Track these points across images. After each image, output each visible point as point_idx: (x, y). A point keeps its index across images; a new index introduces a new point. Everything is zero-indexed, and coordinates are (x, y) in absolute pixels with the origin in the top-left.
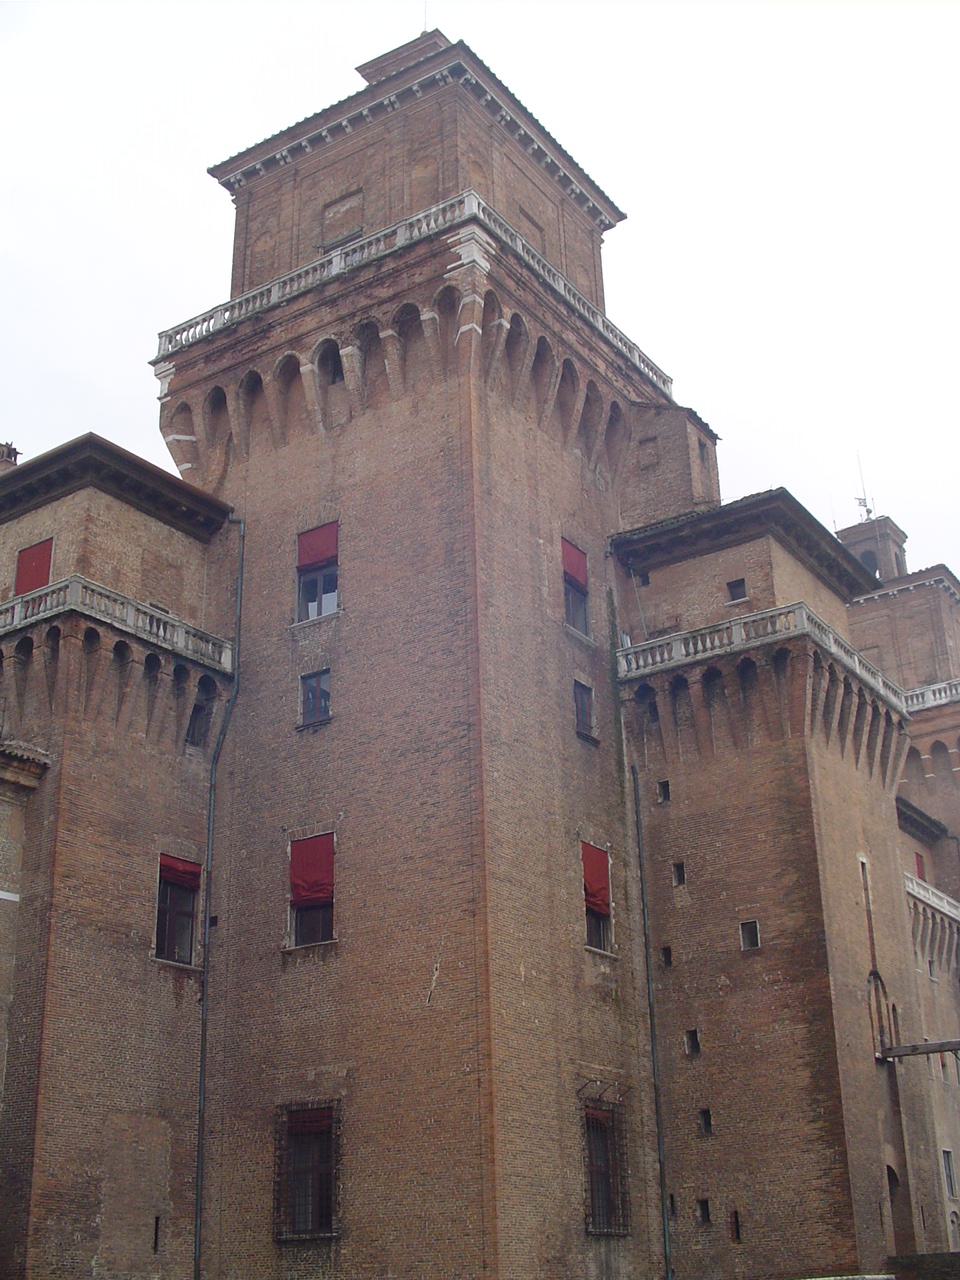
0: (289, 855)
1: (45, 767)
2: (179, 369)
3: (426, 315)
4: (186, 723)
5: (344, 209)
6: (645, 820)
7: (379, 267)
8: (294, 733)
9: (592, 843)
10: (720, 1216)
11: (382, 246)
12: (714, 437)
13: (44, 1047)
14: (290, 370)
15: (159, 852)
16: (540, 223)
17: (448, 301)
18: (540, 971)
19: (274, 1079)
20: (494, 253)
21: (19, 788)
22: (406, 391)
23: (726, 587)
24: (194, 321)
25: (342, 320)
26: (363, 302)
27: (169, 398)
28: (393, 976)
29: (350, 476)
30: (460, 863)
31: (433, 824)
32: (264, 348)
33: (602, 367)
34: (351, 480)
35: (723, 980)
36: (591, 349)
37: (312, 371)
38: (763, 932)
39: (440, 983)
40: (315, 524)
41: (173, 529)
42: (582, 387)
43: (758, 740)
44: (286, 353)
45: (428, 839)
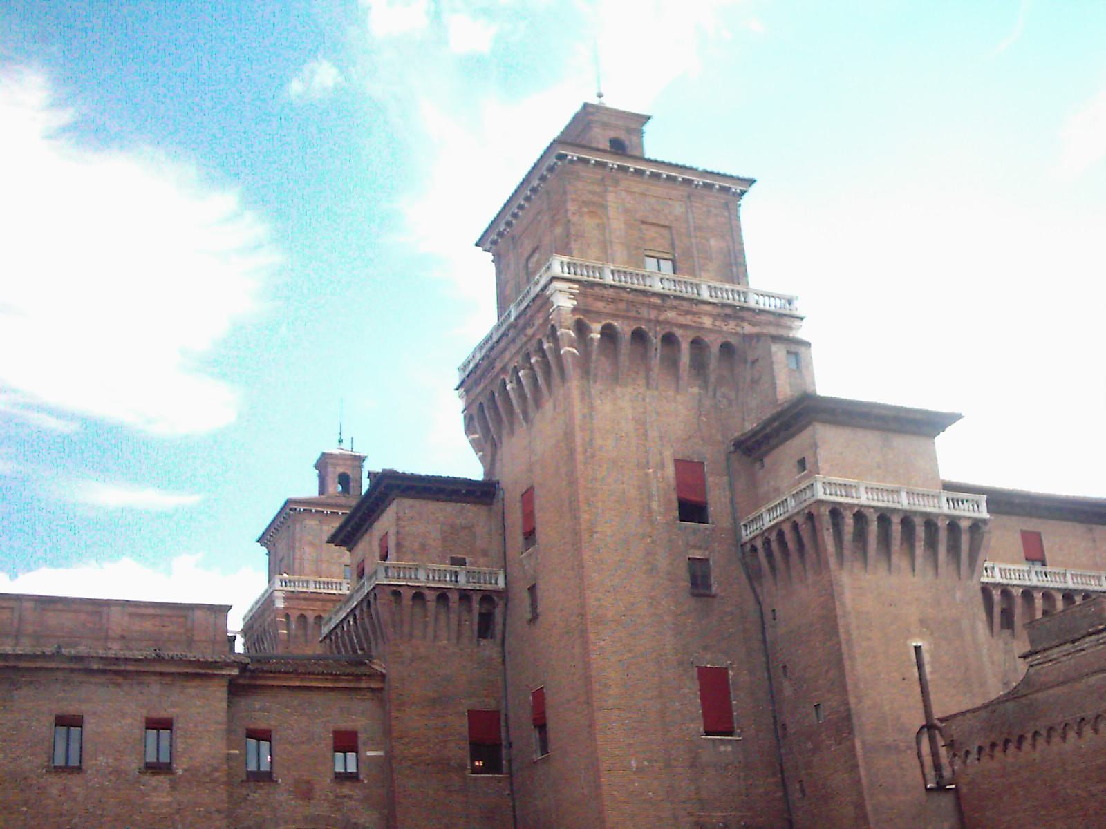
1: (383, 675)
2: (467, 392)
4: (476, 627)
9: (709, 666)
12: (808, 344)
15: (466, 710)
16: (667, 224)
18: (650, 760)
20: (578, 291)
21: (372, 690)
23: (796, 463)
26: (524, 339)
33: (707, 322)
36: (694, 314)
37: (513, 388)
41: (464, 505)
42: (685, 346)
44: (502, 377)
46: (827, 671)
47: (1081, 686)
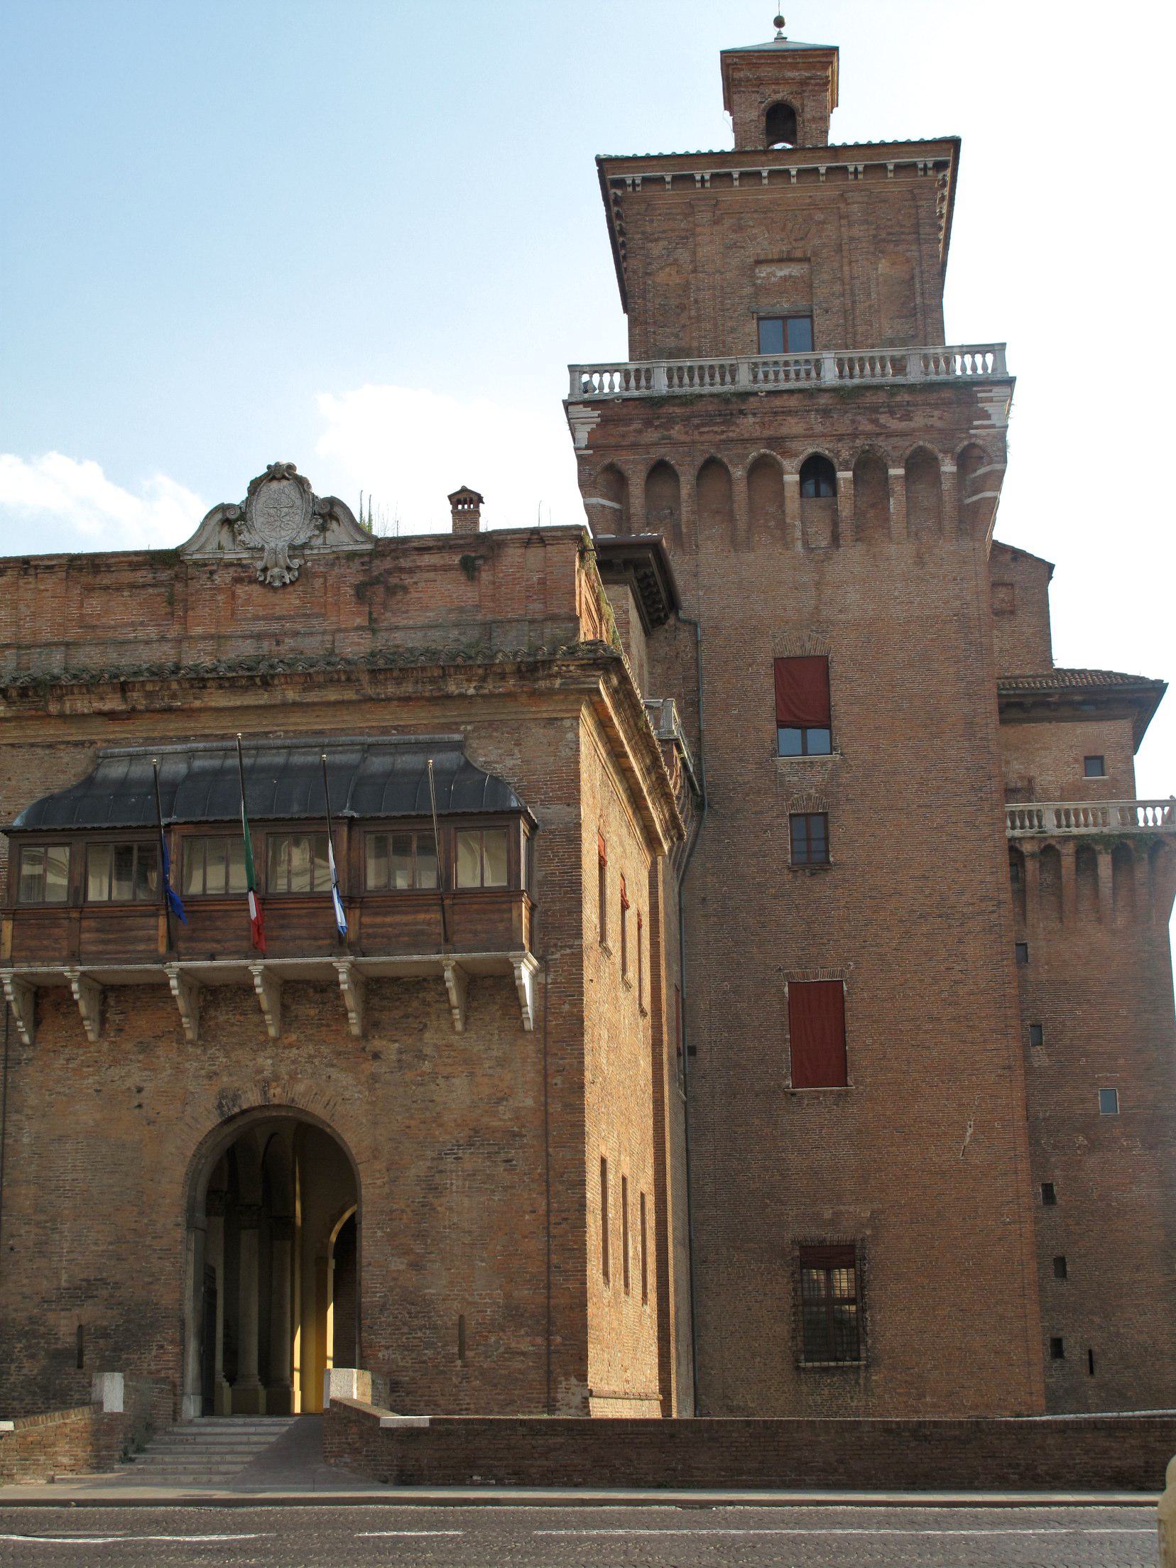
2: (605, 422)
3: (948, 467)
5: (780, 274)
7: (893, 395)
8: (786, 871)
10: (1074, 1352)
14: (764, 469)
19: (782, 1214)
25: (840, 438)
27: (591, 452)
29: (840, 611)
30: (994, 1031)
32: (731, 434)
35: (1081, 1139)
38: (1121, 1101)
39: (974, 1139)
43: (1120, 922)
44: (762, 451)
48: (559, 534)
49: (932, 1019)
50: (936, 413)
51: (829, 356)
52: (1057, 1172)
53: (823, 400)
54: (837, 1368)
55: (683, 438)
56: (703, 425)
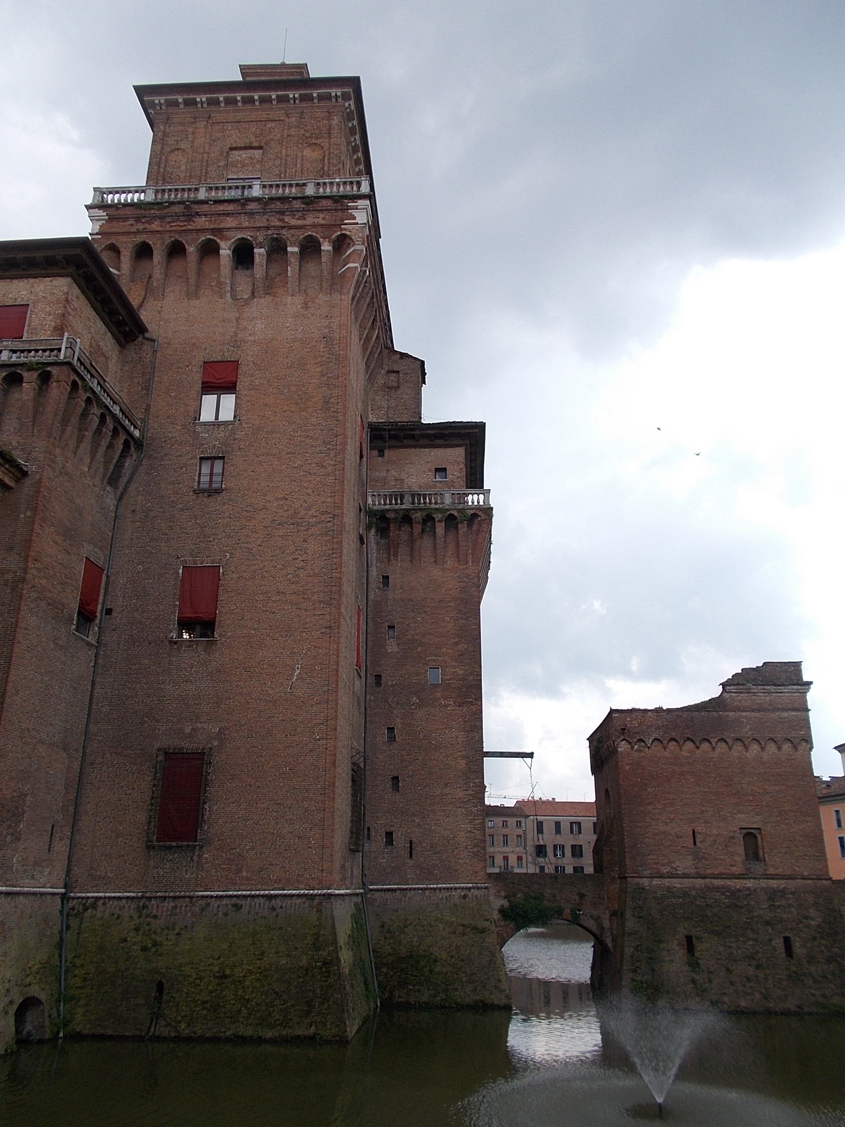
0: (181, 575)
1: (25, 474)
2: (111, 219)
3: (326, 247)
6: (372, 596)
8: (192, 493)
10: (400, 841)
11: (294, 190)
13: (8, 688)
14: (210, 250)
17: (341, 243)
19: (155, 729)
22: (299, 292)
24: (128, 189)
27: (100, 236)
28: (263, 669)
30: (321, 602)
31: (302, 573)
32: (189, 227)
34: (252, 338)
38: (442, 675)
39: (300, 678)
40: (220, 359)
44: (208, 237)
45: (298, 582)
46: (456, 644)
47: (775, 715)
48: (39, 255)
49: (279, 593)
50: (321, 216)
51: (257, 183)
52: (398, 720)
53: (252, 206)
54: (178, 847)
55: (159, 229)
56: (174, 222)
